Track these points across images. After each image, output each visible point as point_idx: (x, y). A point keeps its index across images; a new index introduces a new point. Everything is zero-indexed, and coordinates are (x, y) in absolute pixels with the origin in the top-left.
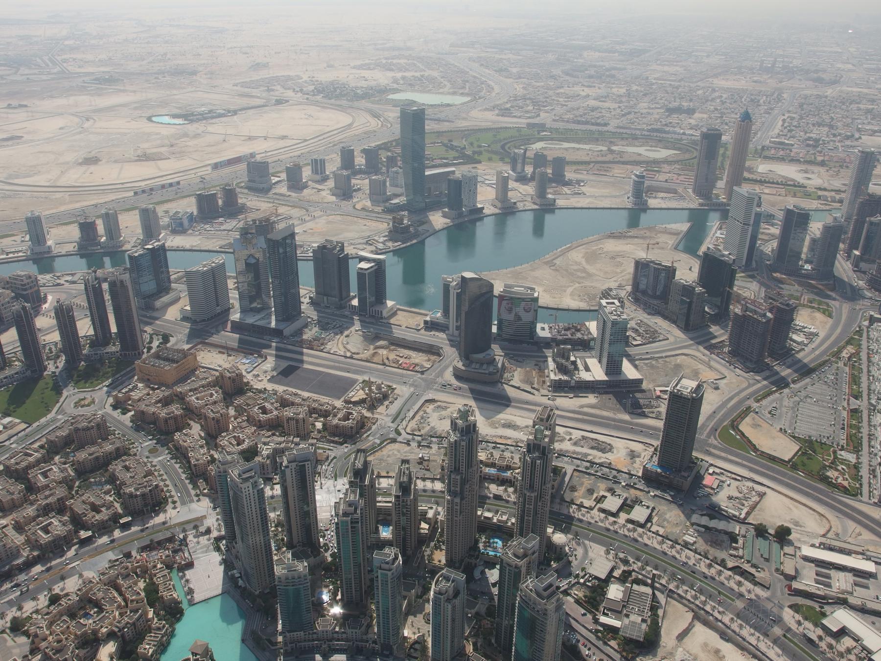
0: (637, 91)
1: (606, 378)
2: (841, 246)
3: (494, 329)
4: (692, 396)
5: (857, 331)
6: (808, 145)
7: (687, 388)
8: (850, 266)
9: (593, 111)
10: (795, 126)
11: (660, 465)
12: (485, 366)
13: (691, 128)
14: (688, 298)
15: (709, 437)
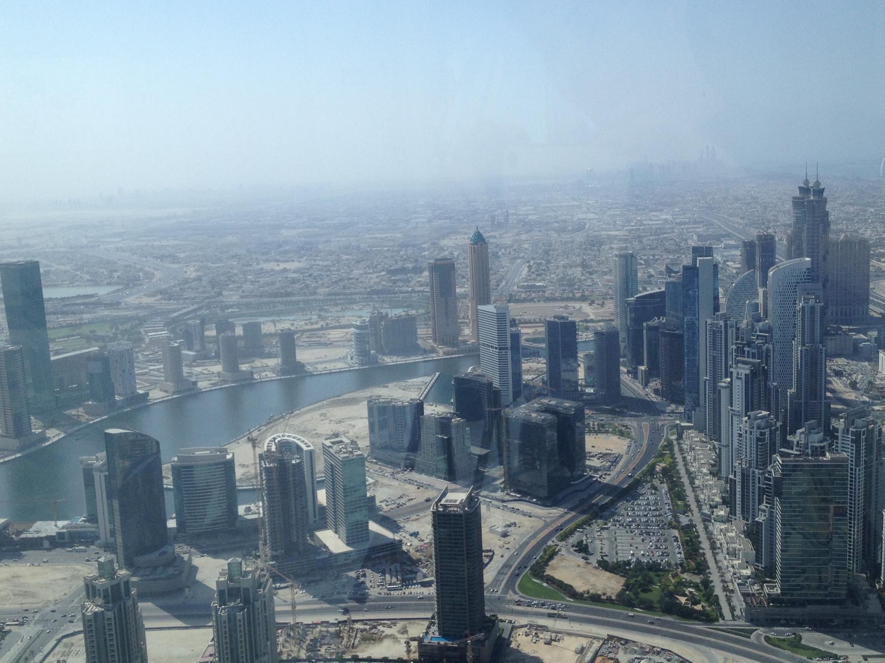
0: (347, 259)
1: (349, 549)
2: (623, 369)
3: (172, 524)
4: (465, 511)
5: (666, 446)
6: (563, 285)
7: (455, 501)
8: (640, 386)
9: (294, 283)
10: (544, 270)
11: (444, 634)
12: (160, 570)
13: (421, 285)
14: (446, 436)
15: (506, 593)
